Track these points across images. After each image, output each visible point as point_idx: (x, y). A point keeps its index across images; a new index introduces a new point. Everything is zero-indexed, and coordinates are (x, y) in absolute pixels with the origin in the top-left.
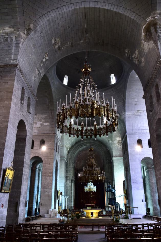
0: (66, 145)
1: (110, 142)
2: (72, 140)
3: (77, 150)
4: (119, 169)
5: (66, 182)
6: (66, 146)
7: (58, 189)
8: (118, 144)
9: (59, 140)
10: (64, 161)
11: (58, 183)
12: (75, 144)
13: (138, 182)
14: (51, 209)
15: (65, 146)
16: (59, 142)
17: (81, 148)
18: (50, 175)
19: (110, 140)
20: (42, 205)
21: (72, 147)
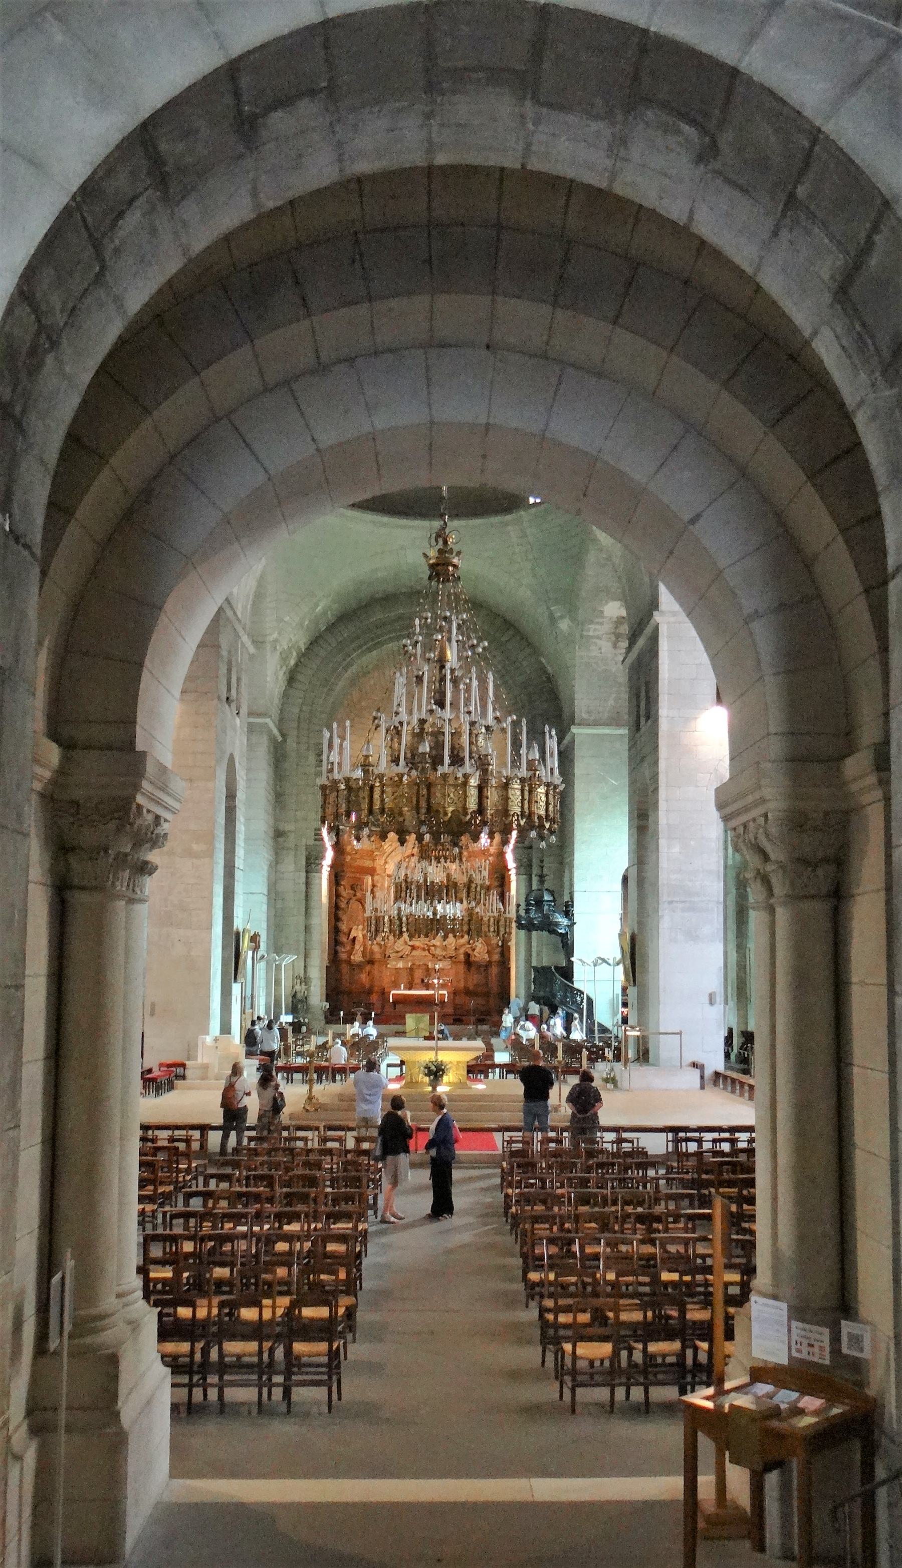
0: (275, 635)
1: (564, 625)
2: (317, 605)
3: (346, 669)
5: (277, 863)
6: (276, 641)
7: (239, 923)
8: (610, 644)
9: (241, 633)
10: (265, 740)
11: (239, 888)
12: (332, 628)
13: (696, 899)
14: (208, 1034)
15: (268, 647)
16: (245, 638)
17: (370, 650)
18: (195, 847)
19: (562, 617)
20: (152, 1014)
21: (315, 642)
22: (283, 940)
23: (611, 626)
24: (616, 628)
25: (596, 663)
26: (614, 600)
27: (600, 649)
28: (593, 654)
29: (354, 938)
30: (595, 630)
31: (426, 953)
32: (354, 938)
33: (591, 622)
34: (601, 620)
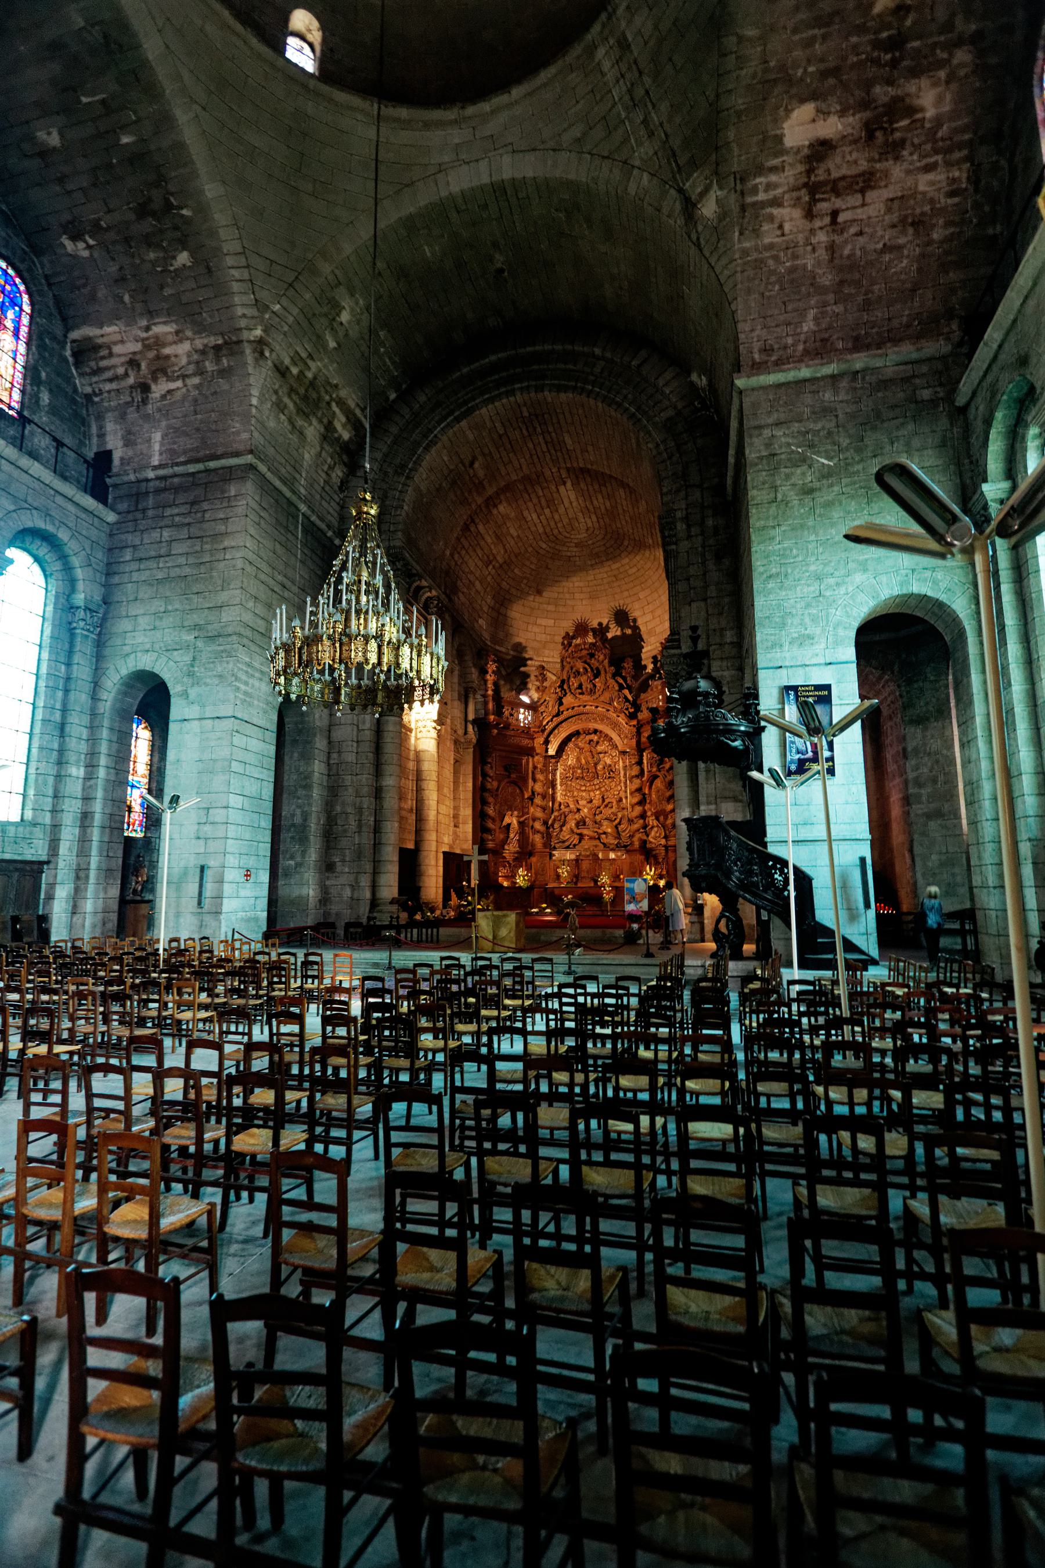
0: (258, 332)
4: (808, 491)
6: (261, 342)
8: (797, 213)
22: (338, 809)
23: (801, 168)
24: (809, 172)
25: (776, 258)
26: (803, 101)
27: (781, 227)
28: (767, 241)
29: (509, 825)
30: (769, 187)
31: (597, 842)
32: (509, 825)
33: (761, 170)
34: (776, 162)
